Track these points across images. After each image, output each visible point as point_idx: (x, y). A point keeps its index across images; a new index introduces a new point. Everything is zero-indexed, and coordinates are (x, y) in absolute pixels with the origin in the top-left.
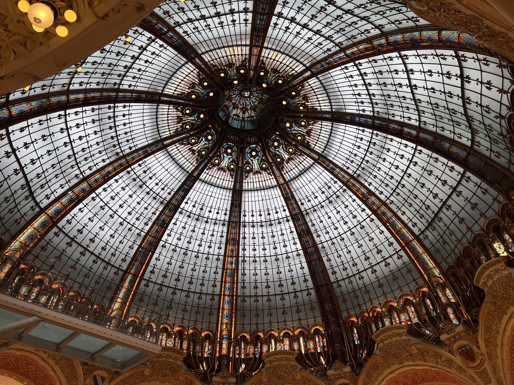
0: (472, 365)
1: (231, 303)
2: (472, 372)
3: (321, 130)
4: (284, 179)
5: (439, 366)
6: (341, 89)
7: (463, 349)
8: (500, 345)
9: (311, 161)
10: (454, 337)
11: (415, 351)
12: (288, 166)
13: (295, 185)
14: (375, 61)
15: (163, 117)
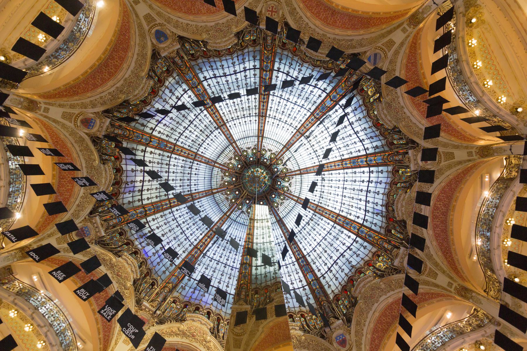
0: (81, 118)
1: (266, 42)
2: (76, 111)
3: (217, 181)
4: (233, 146)
5: (98, 96)
6: (212, 210)
7: (92, 124)
8: (74, 144)
9: (219, 161)
10: (102, 127)
11: (120, 96)
12: (231, 155)
13: (226, 142)
14: (201, 234)
15: (298, 187)
